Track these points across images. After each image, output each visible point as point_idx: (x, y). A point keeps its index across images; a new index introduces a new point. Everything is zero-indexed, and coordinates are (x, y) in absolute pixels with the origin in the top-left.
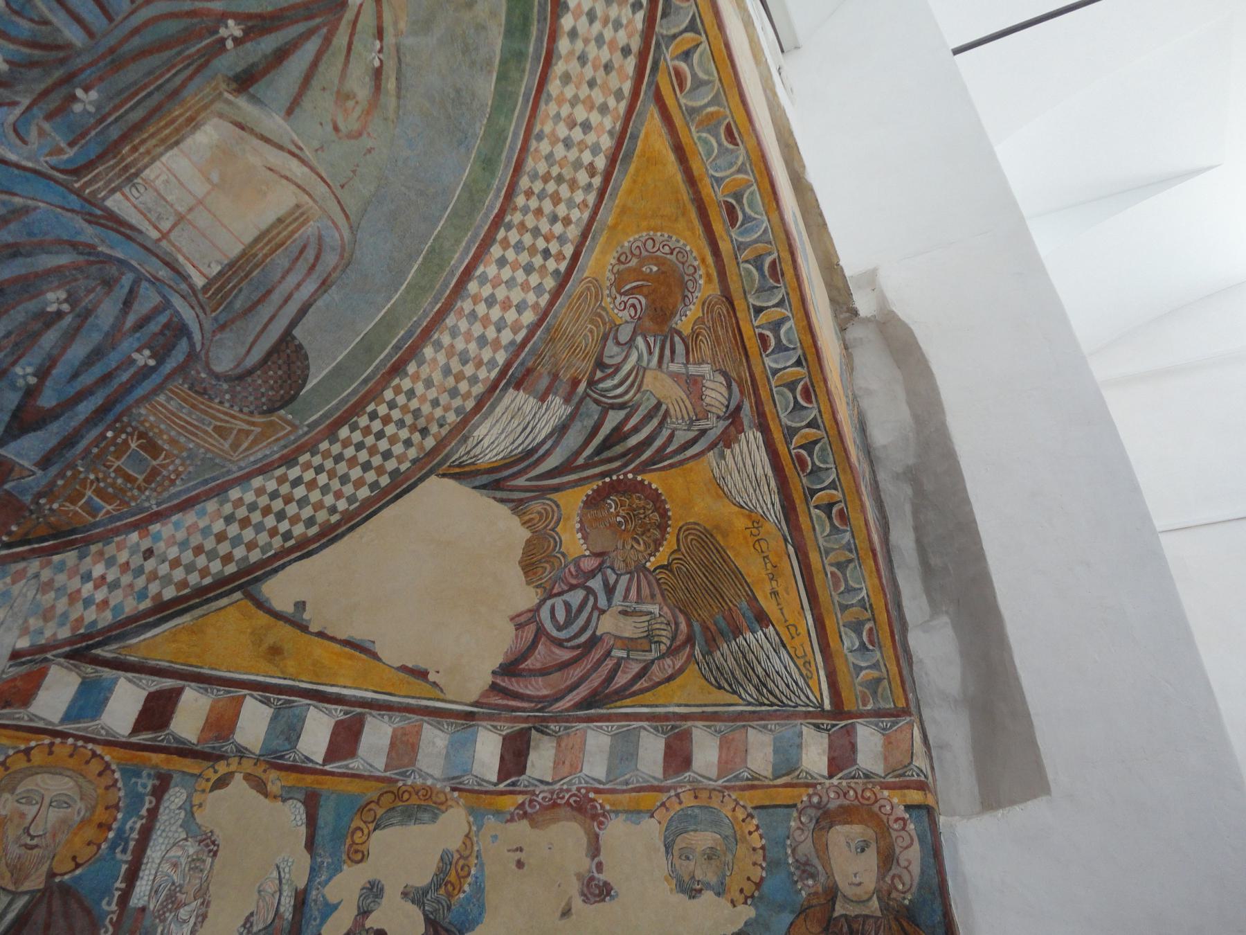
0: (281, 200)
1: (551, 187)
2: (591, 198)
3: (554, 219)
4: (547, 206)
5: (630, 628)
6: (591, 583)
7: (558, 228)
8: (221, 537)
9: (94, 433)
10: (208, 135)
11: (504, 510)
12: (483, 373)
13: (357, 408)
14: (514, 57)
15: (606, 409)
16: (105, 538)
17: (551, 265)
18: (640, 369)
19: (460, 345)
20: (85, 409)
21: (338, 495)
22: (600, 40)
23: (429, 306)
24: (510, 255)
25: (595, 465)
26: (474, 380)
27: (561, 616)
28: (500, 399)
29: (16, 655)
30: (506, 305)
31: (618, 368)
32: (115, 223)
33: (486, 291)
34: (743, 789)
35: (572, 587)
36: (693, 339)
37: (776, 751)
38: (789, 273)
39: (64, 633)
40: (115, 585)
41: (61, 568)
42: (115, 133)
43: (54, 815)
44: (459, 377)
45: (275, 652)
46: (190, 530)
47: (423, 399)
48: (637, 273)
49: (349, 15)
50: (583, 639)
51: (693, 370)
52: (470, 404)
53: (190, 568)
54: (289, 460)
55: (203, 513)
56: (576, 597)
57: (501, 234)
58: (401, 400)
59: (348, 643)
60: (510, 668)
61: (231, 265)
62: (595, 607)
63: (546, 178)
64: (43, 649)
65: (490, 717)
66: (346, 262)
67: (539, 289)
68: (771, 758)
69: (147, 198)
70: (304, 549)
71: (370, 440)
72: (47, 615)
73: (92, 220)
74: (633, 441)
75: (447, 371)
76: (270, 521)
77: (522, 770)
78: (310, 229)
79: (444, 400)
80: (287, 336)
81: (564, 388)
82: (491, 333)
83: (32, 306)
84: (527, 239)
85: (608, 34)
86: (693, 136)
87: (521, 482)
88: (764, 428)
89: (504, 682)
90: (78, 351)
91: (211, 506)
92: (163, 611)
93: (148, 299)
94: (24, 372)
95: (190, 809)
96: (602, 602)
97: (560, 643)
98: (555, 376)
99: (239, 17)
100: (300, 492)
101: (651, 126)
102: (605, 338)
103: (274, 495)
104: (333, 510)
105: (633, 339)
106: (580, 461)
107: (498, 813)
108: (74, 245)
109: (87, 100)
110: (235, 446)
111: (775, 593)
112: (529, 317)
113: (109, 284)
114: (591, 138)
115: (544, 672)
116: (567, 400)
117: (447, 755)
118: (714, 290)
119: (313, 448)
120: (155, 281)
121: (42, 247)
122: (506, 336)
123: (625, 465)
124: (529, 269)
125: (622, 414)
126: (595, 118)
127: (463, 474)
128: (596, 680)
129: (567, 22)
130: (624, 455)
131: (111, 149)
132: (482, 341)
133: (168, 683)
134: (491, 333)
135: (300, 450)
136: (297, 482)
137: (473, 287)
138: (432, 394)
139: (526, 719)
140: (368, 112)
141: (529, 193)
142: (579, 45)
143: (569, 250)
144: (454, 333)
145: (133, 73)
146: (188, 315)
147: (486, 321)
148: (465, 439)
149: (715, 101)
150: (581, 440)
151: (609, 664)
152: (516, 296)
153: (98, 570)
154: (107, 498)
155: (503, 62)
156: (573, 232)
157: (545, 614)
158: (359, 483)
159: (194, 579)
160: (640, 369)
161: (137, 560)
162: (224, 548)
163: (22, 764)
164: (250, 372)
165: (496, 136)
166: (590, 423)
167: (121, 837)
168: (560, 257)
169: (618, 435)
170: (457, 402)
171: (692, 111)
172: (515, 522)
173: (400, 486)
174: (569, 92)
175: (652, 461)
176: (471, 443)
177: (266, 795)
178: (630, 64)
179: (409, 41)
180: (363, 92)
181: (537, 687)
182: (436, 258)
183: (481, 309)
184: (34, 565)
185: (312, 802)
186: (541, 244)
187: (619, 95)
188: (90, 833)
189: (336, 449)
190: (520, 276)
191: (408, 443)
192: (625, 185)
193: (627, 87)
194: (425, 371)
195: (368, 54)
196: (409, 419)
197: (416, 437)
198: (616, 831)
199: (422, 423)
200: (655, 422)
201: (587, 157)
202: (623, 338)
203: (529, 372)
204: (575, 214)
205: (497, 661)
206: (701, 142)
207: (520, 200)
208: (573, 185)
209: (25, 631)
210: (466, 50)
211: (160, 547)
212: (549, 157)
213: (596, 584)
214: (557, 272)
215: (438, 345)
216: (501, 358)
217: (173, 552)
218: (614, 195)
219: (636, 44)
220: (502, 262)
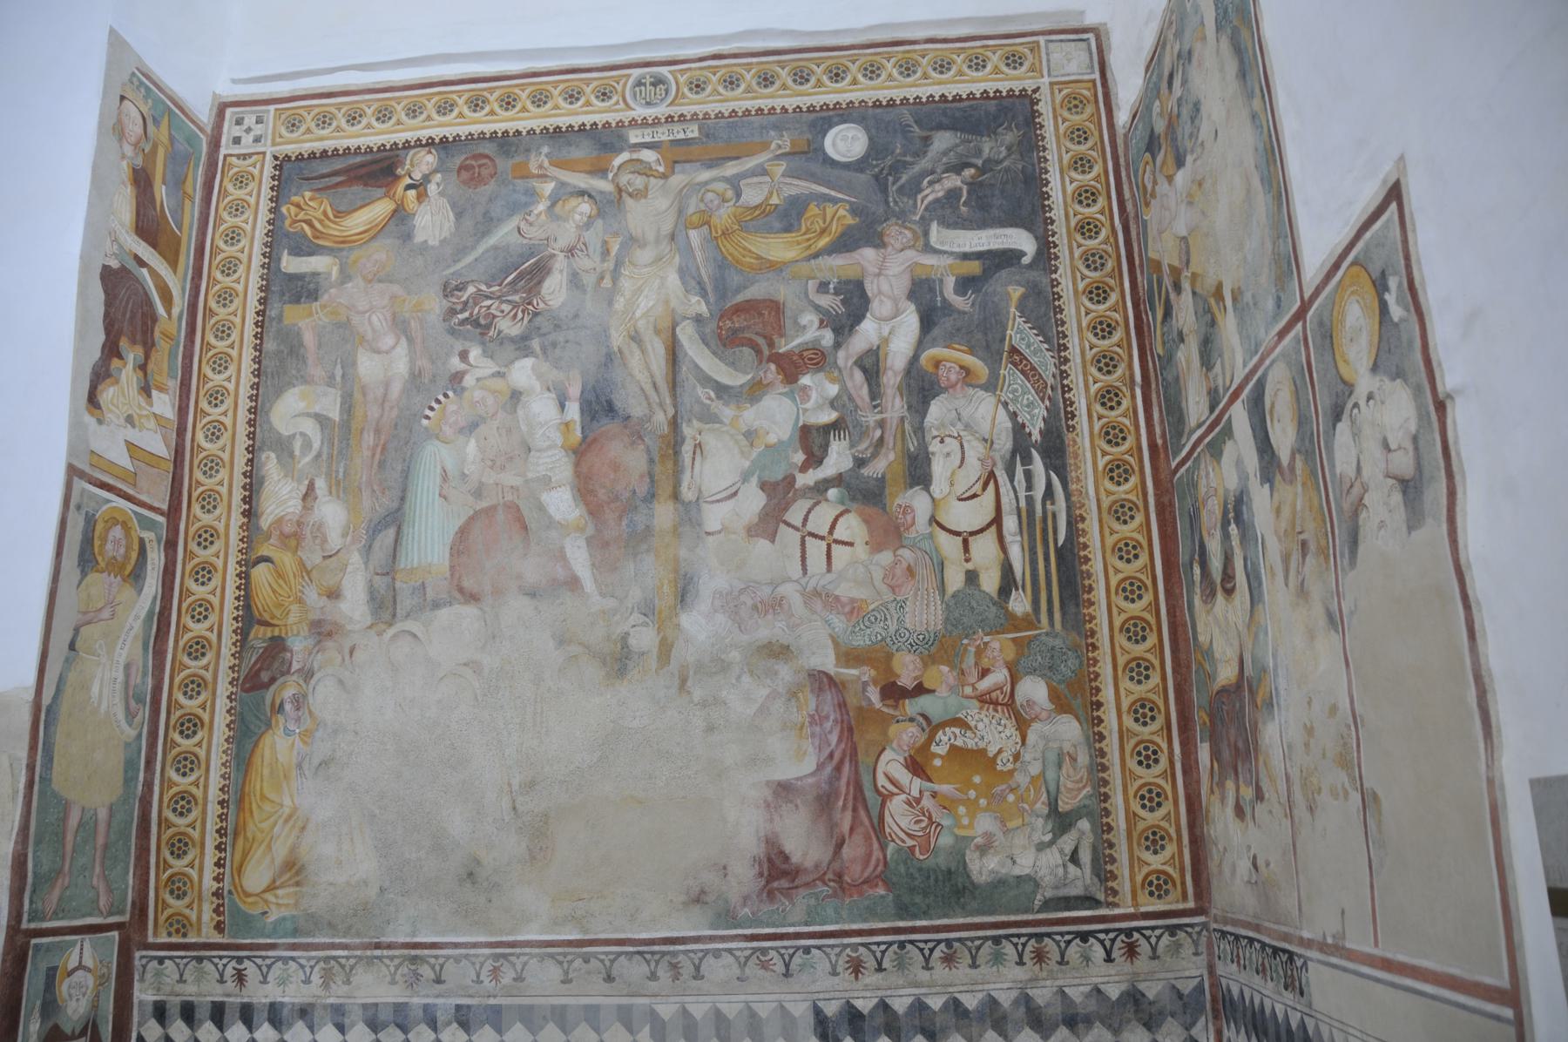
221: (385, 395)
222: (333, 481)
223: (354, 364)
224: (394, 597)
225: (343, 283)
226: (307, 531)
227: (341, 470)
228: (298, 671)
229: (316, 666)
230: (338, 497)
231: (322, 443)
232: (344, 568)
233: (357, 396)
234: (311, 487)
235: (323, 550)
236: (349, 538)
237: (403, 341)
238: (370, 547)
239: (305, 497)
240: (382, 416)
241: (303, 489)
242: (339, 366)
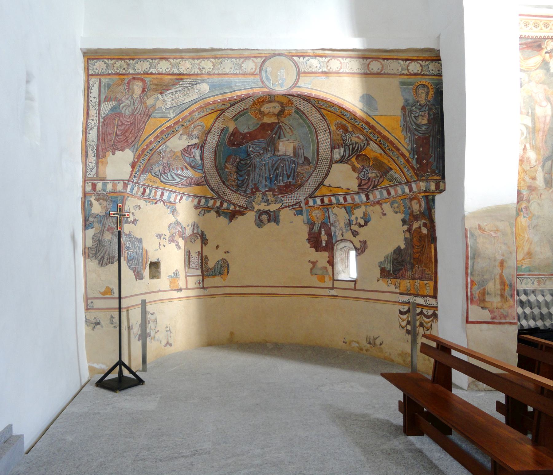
0: (292, 145)
1: (319, 124)
2: (325, 122)
3: (322, 127)
4: (320, 126)
5: (374, 175)
6: (364, 170)
7: (324, 127)
8: (315, 180)
9: (295, 174)
10: (281, 144)
11: (345, 164)
12: (329, 150)
13: (318, 161)
14: (301, 116)
15: (349, 146)
16: (304, 184)
17: (327, 132)
18: (350, 138)
19: (323, 148)
20: (293, 173)
21: (324, 170)
22: (307, 108)
23: (316, 145)
24: (321, 134)
25: (354, 153)
26: (328, 151)
27: (363, 176)
28: (333, 152)
29: (304, 199)
30: (325, 140)
31: (346, 139)
32: (280, 155)
33: (321, 140)
34: (399, 197)
35: (362, 172)
36: (353, 131)
37: (401, 190)
38: (357, 118)
39: (307, 196)
40: (309, 189)
41: (302, 189)
42: (274, 149)
43: (318, 215)
44: (326, 151)
45: (331, 191)
46: (312, 180)
47: (324, 156)
48: (338, 127)
49: (282, 126)
50: (368, 178)
51: (357, 135)
52: (330, 154)
53: (315, 184)
54: (315, 169)
55: (312, 178)
56: (363, 173)
57: (317, 132)
58: (322, 157)
59: (337, 187)
60: (360, 185)
61: (293, 153)
62: (367, 173)
63: (317, 123)
64: (307, 197)
65: (361, 193)
66: (303, 147)
67: (328, 136)
68: (401, 191)
69: (281, 152)
70: (325, 178)
71: (322, 163)
72: (305, 194)
73: (279, 156)
74: (356, 148)
75: (324, 152)
76: (319, 176)
77: (369, 199)
78: (297, 146)
79: (327, 155)
80: (305, 157)
81: (341, 146)
82: (326, 144)
83: (281, 166)
84: (321, 131)
85: (308, 107)
86: (329, 109)
87: (345, 160)
88: (372, 140)
89: (360, 188)
90: (288, 168)
91: (312, 177)
92: (316, 190)
93: (289, 160)
94: (285, 172)
95: (332, 211)
96: (367, 173)
97: (365, 180)
98: (338, 145)
99: (274, 134)
100: (320, 172)
101: (323, 111)
102: (341, 137)
103: (317, 173)
104: (325, 172)
105: (345, 135)
106: (351, 154)
107: (368, 205)
108: (279, 160)
109: (270, 149)
110: (309, 170)
111: (391, 165)
112: (329, 140)
113: (285, 161)
114: (317, 117)
115: (365, 185)
116: (342, 147)
117: (359, 199)
118: (350, 124)
119: (316, 167)
120: (288, 158)
121: (277, 161)
122: (328, 144)
123: (357, 152)
124: (324, 134)
125: (352, 145)
126: (315, 115)
127: (337, 162)
128: (373, 184)
129: (302, 110)
130: (356, 151)
131: (275, 150)
132: (325, 146)
133: (322, 197)
134: (326, 144)
135: (316, 167)
136: (318, 171)
137: (319, 140)
138: (325, 155)
139: (366, 192)
140: (292, 131)
141: (317, 126)
142: (306, 110)
143: (328, 129)
144: (321, 147)
145: (271, 144)
146: (294, 159)
147: (324, 143)
148: (333, 158)
149: (327, 105)
150: (348, 151)
151: (373, 181)
152: (325, 138)
153: (306, 188)
154: (302, 180)
155: (300, 117)
156: (326, 126)
157: (360, 176)
158: (325, 168)
159: (316, 185)
160: (350, 138)
161: (309, 185)
162: (317, 181)
163: (312, 210)
164: (304, 162)
165: (307, 124)
166: (348, 148)
167: (326, 216)
168: (327, 130)
169: (353, 149)
170: (328, 154)
171: (326, 107)
172: (348, 165)
173: (330, 167)
174: (310, 115)
175: (361, 150)
176: (334, 158)
177: (339, 208)
178: (313, 108)
179: (289, 123)
180: (290, 131)
181: (365, 187)
182: (312, 140)
183: (322, 142)
184: (300, 190)
185: (345, 208)
186: (323, 130)
187: (315, 111)
188: (323, 216)
189: (319, 166)
190: (324, 135)
191: (327, 161)
192: (327, 118)
193: (316, 110)
194: (321, 153)
195: (287, 127)
196: (325, 159)
197: (327, 160)
198: (384, 206)
199: (327, 158)
200: (357, 144)
201: (319, 119)
202: (344, 135)
203: (334, 146)
204: (324, 124)
205: (357, 185)
206: (331, 109)
207: (316, 127)
208: (321, 122)
209: (304, 196)
210: (296, 119)
211: (310, 183)
212: (315, 121)
213: (364, 170)
214: (328, 132)
215: (321, 149)
216: (330, 146)
217: (312, 183)
218: (327, 119)
219: (312, 106)
220: (320, 135)
221: (545, 120)
222: (532, 145)
223: (534, 109)
224: (552, 181)
225: (529, 82)
226: (525, 160)
227: (534, 142)
228: (525, 200)
229: (531, 199)
230: (533, 150)
231: (527, 133)
232: (536, 171)
233: (537, 120)
234: (525, 147)
235: (530, 166)
236: (537, 163)
237: (549, 104)
238: (544, 166)
239: (524, 149)
240: (544, 127)
241: (523, 147)
242: (530, 110)
